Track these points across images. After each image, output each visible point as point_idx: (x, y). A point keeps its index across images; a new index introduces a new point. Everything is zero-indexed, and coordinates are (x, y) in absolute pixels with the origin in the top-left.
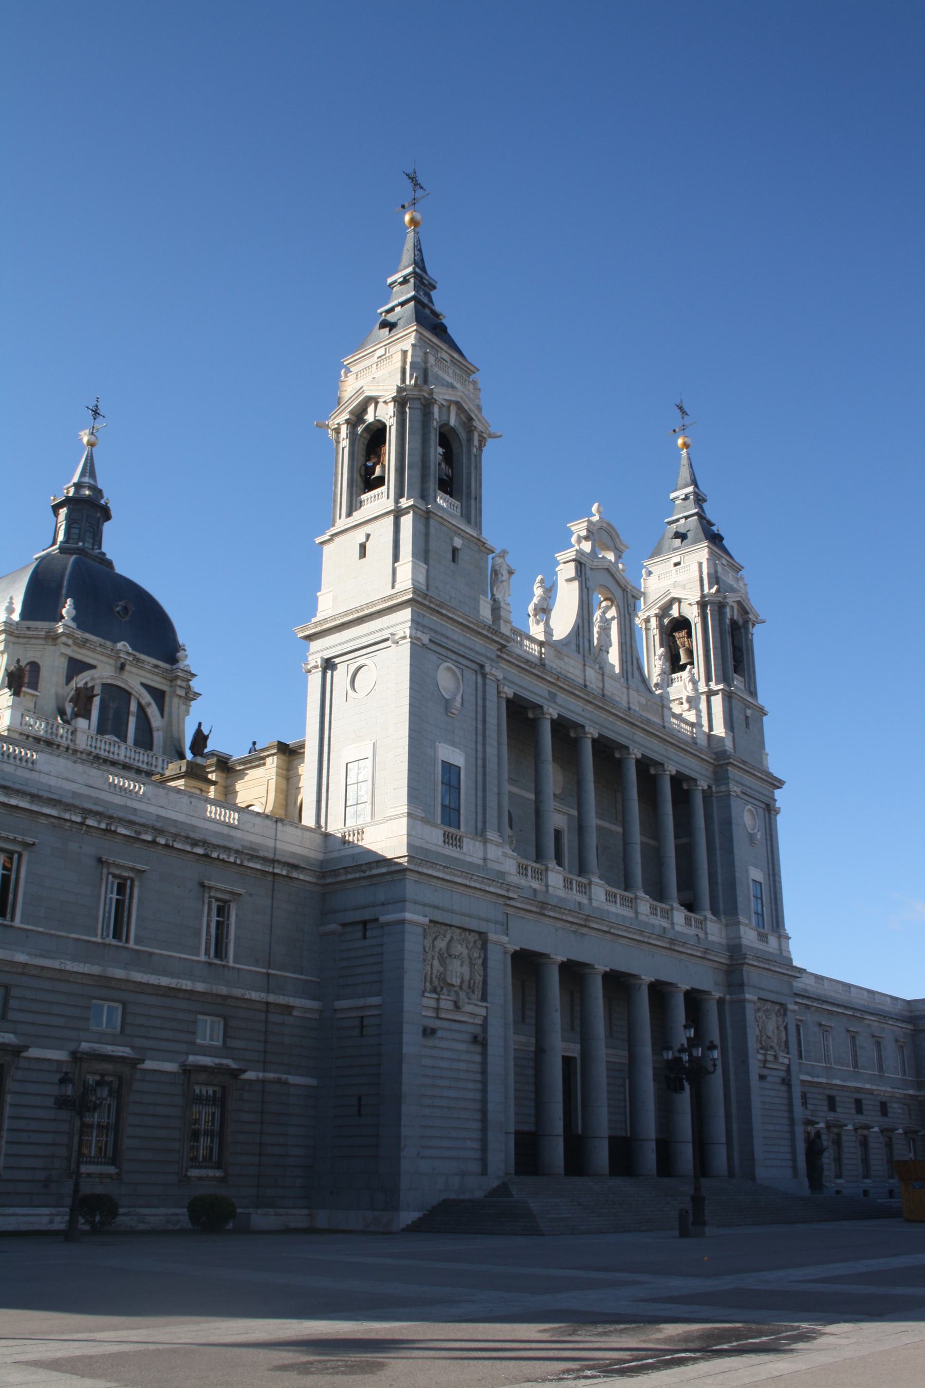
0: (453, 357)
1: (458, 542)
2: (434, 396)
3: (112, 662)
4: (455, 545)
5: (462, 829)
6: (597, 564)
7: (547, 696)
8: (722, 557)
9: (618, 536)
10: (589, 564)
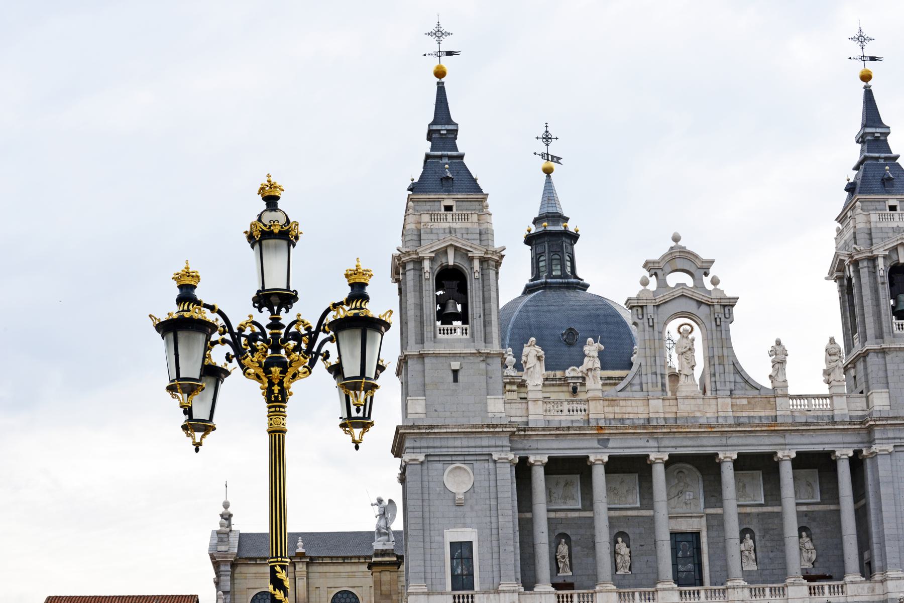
0: (458, 198)
1: (455, 365)
2: (420, 255)
3: (565, 389)
4: (453, 368)
5: (477, 588)
6: (661, 299)
7: (596, 444)
8: (888, 199)
9: (696, 256)
10: (651, 303)
